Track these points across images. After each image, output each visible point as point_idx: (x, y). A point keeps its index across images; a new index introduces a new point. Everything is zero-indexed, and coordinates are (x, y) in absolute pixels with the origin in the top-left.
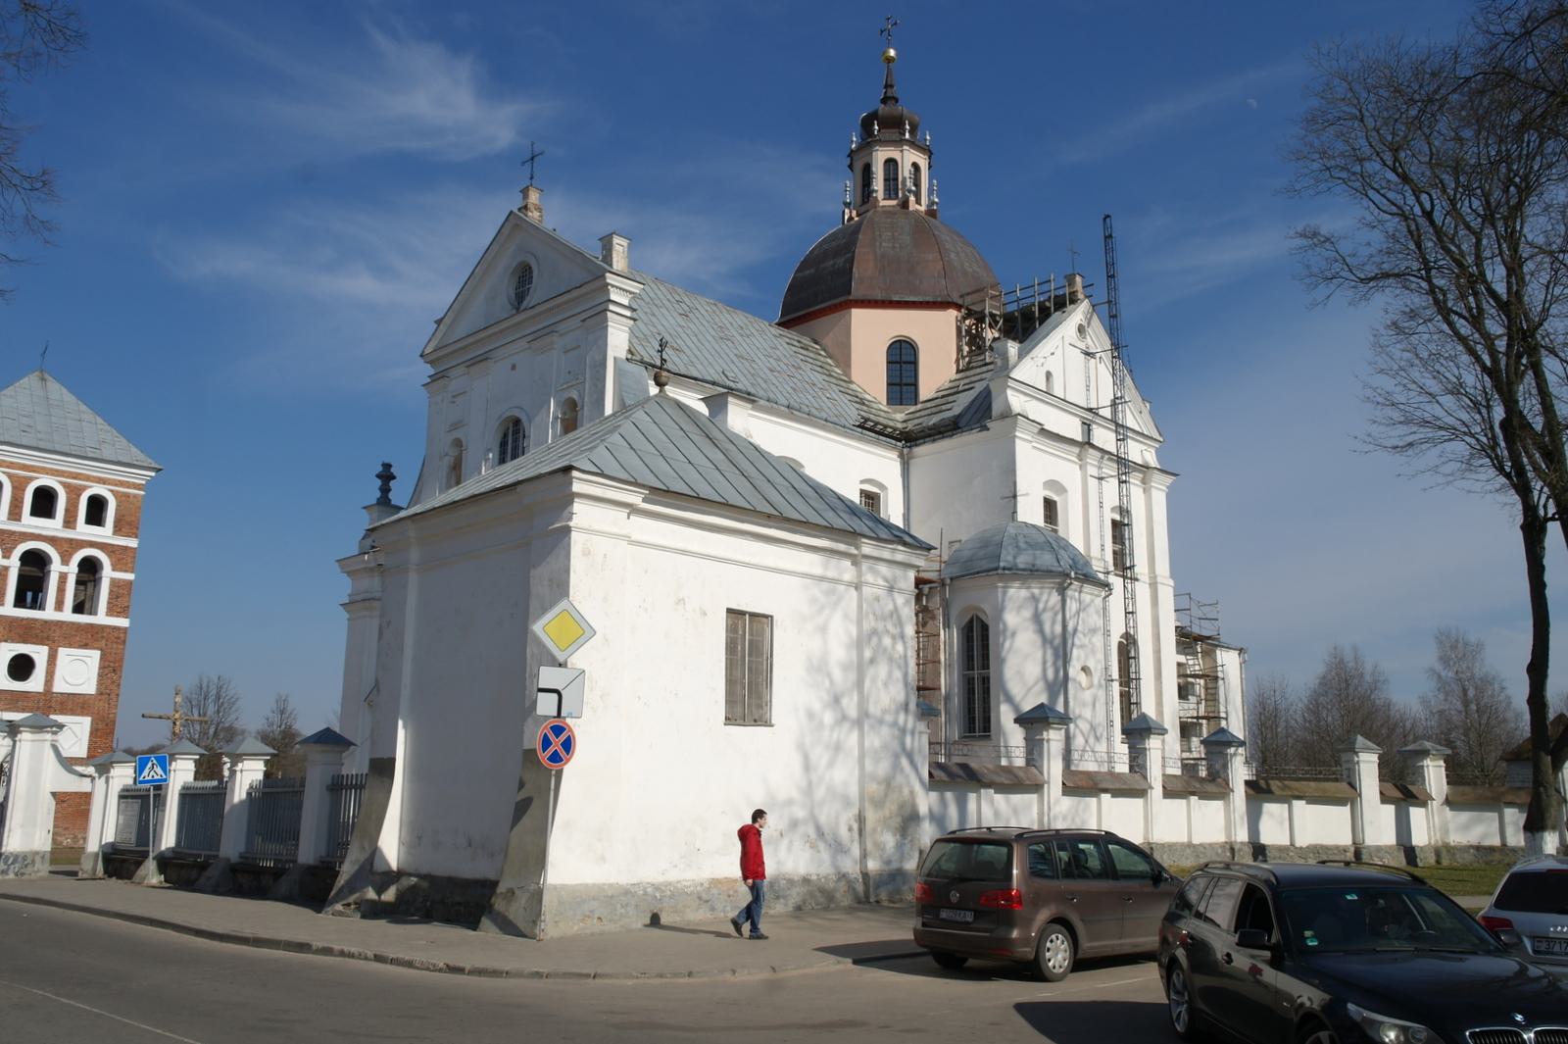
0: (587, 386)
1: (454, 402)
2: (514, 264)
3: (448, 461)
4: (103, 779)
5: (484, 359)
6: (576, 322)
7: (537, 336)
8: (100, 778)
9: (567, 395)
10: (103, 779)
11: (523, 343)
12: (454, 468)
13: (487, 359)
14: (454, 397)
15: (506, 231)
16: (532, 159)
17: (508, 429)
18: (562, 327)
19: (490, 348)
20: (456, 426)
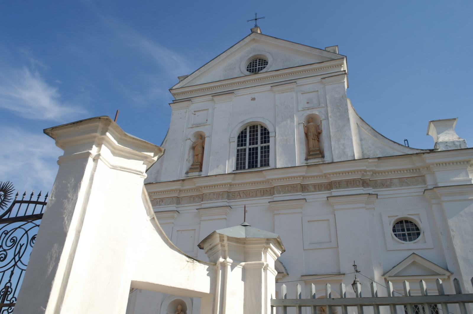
0: (329, 109)
1: (195, 114)
2: (250, 56)
3: (189, 144)
4: (239, 269)
5: (231, 92)
6: (319, 78)
7: (275, 85)
8: (233, 268)
9: (309, 112)
10: (239, 269)
11: (268, 87)
12: (193, 148)
13: (233, 93)
14: (195, 111)
15: (247, 40)
16: (256, 19)
17: (246, 129)
18: (299, 82)
19: (234, 89)
20: (198, 126)
